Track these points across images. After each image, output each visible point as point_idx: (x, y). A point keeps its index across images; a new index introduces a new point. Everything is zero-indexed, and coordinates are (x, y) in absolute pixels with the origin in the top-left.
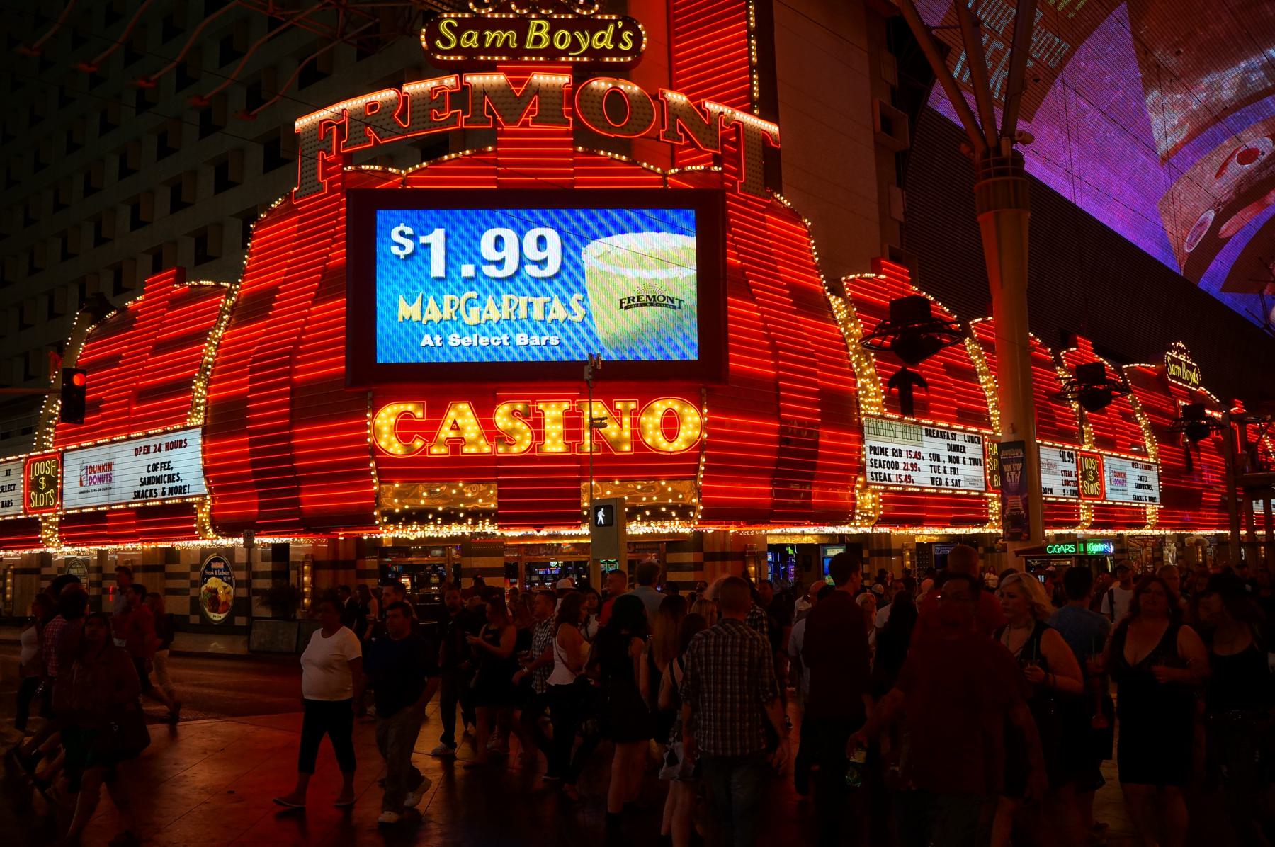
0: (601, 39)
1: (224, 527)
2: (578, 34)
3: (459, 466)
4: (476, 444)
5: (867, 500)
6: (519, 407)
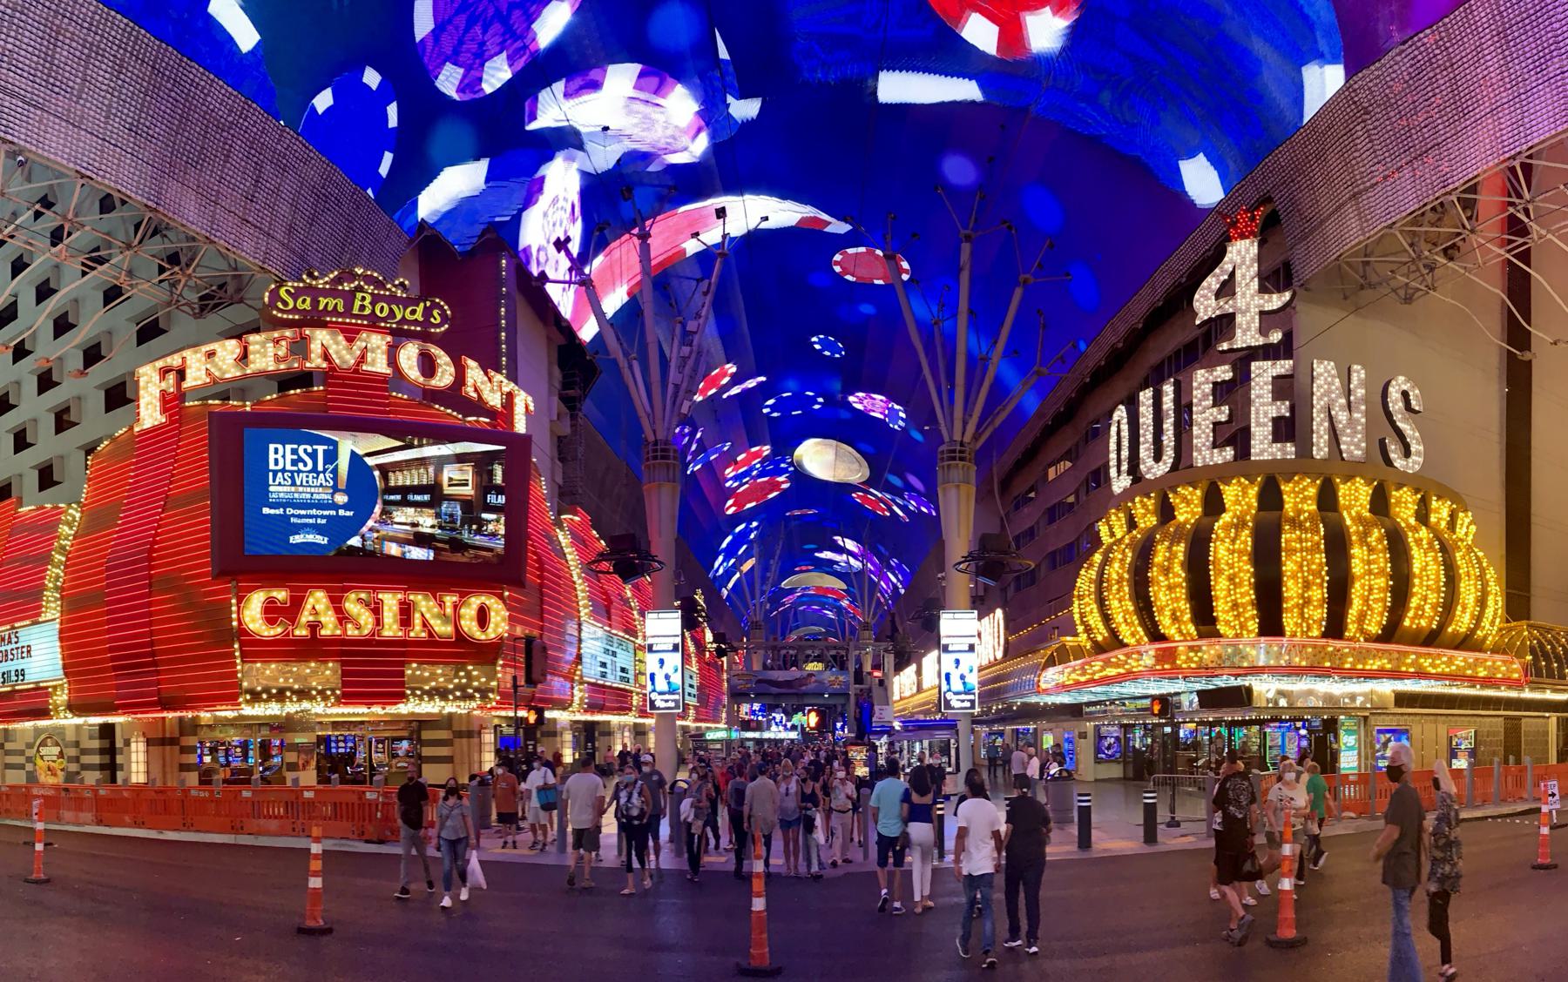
0: (413, 312)
1: (75, 708)
2: (394, 307)
3: (313, 647)
4: (329, 628)
5: (578, 694)
6: (363, 596)
